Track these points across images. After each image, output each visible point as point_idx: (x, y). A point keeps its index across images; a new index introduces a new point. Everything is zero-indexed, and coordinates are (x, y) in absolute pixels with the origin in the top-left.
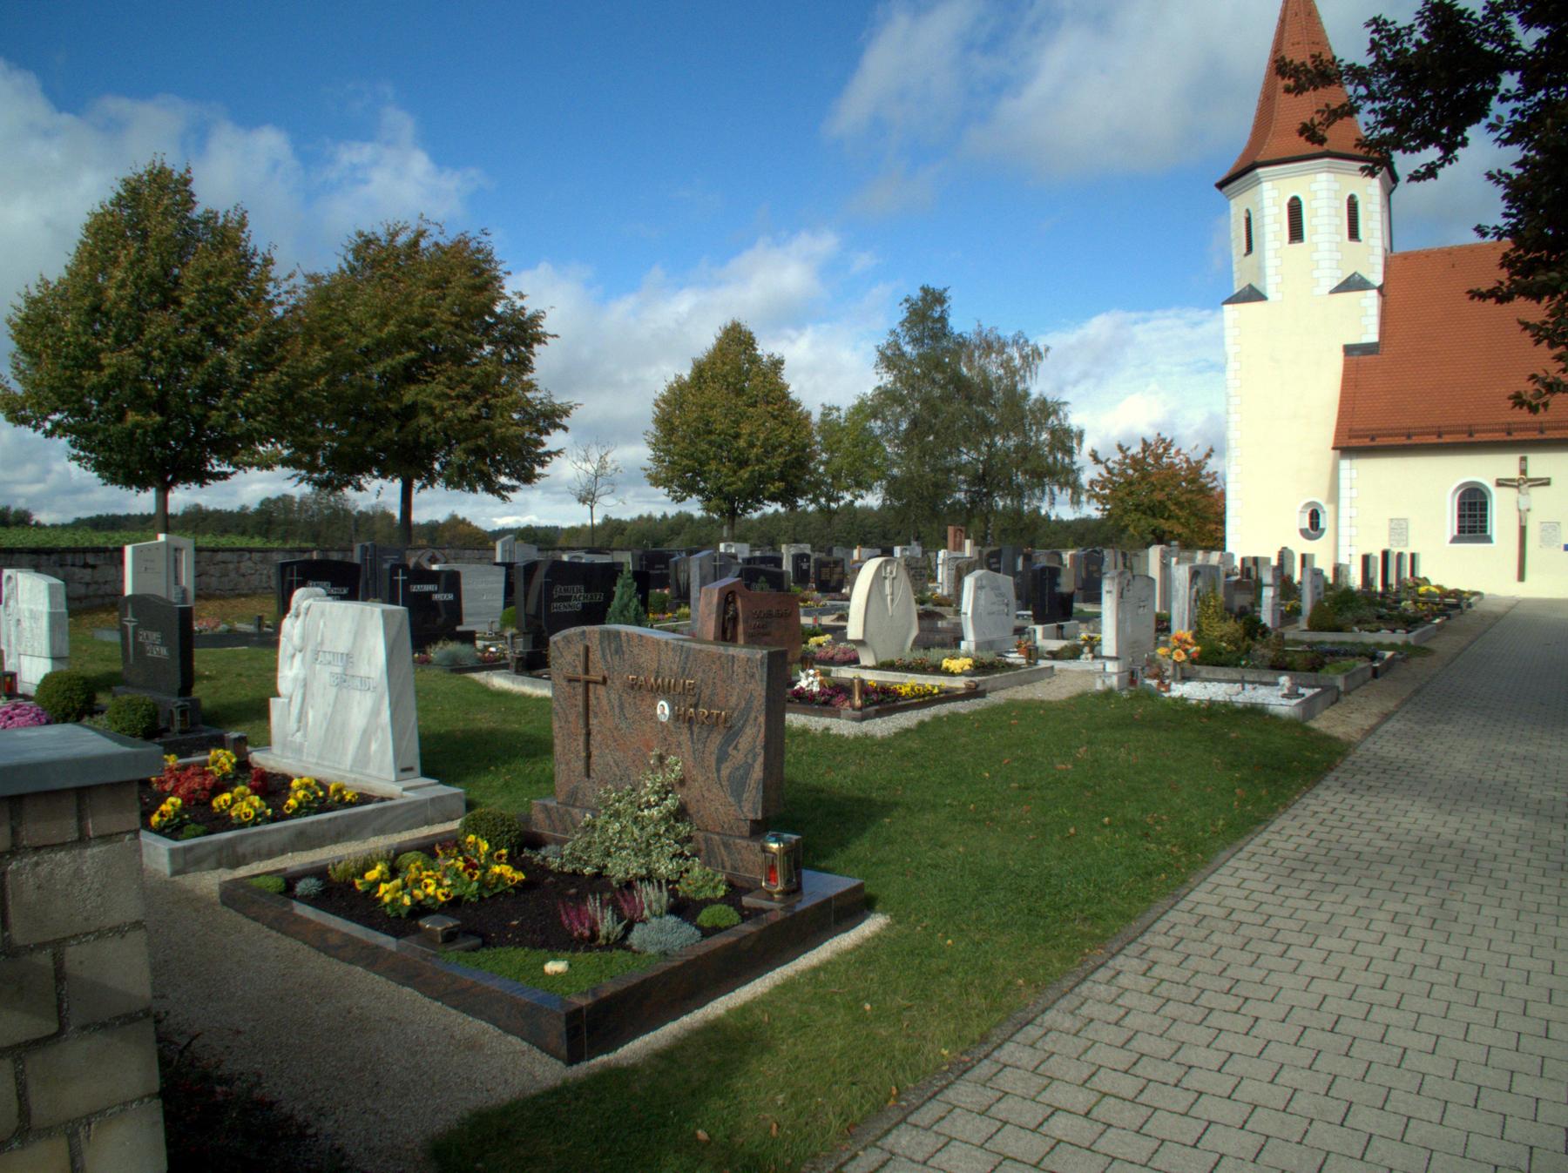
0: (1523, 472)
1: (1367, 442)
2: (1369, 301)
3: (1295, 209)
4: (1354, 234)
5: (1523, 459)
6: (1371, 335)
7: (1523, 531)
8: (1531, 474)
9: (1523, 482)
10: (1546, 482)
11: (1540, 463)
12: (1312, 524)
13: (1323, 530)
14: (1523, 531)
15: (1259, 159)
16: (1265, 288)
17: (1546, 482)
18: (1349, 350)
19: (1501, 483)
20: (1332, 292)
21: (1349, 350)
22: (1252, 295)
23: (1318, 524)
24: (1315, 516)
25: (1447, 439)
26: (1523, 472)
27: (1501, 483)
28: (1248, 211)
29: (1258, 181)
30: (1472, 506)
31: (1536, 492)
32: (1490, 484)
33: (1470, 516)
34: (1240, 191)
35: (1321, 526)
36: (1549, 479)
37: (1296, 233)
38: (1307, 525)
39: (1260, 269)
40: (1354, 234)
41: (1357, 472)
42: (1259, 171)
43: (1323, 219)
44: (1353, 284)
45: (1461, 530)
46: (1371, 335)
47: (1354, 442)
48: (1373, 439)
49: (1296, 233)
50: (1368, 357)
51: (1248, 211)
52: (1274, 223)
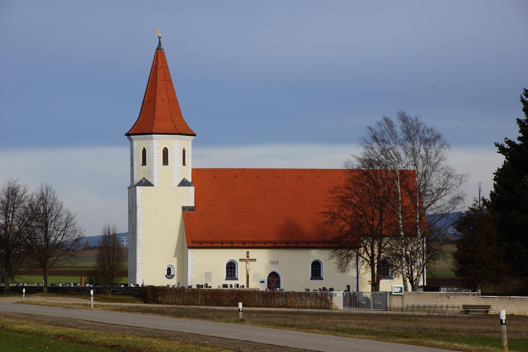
0: (248, 257)
1: (198, 245)
2: (191, 190)
3: (165, 152)
4: (184, 164)
5: (248, 252)
6: (192, 204)
7: (248, 276)
8: (250, 258)
9: (248, 260)
10: (255, 260)
11: (254, 253)
12: (168, 273)
13: (173, 276)
14: (248, 276)
15: (153, 131)
16: (153, 181)
17: (255, 260)
18: (184, 208)
19: (240, 260)
20: (178, 186)
21: (184, 208)
22: (146, 183)
23: (170, 273)
24: (169, 270)
25: (225, 245)
26: (248, 257)
27: (240, 260)
28: (144, 149)
29: (152, 139)
30: (231, 268)
31: (252, 263)
32: (238, 261)
33: (230, 271)
34: (140, 139)
35: (172, 274)
36: (256, 259)
37: (165, 162)
38: (167, 274)
39: (151, 173)
40: (184, 164)
41: (194, 255)
42: (153, 135)
43: (175, 157)
44: (184, 183)
45: (227, 276)
46: (192, 204)
47: (194, 245)
48: (200, 244)
49: (165, 162)
50: (192, 212)
51: (144, 149)
52: (156, 157)
